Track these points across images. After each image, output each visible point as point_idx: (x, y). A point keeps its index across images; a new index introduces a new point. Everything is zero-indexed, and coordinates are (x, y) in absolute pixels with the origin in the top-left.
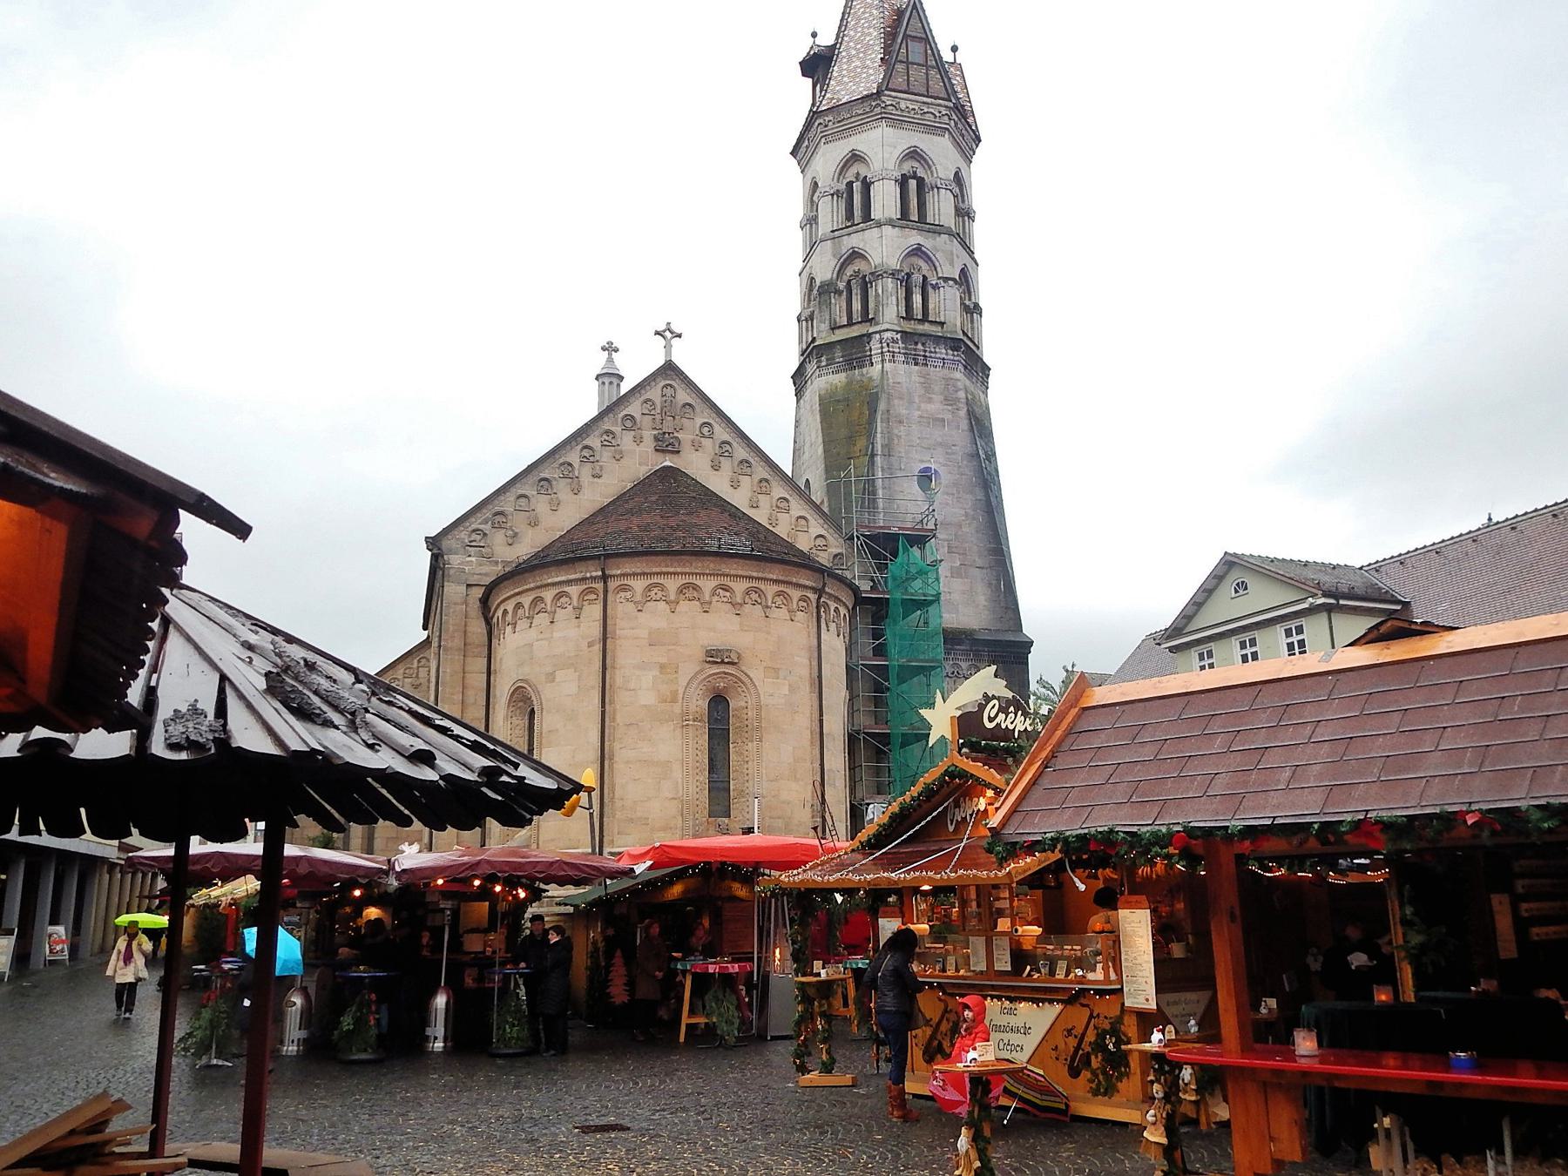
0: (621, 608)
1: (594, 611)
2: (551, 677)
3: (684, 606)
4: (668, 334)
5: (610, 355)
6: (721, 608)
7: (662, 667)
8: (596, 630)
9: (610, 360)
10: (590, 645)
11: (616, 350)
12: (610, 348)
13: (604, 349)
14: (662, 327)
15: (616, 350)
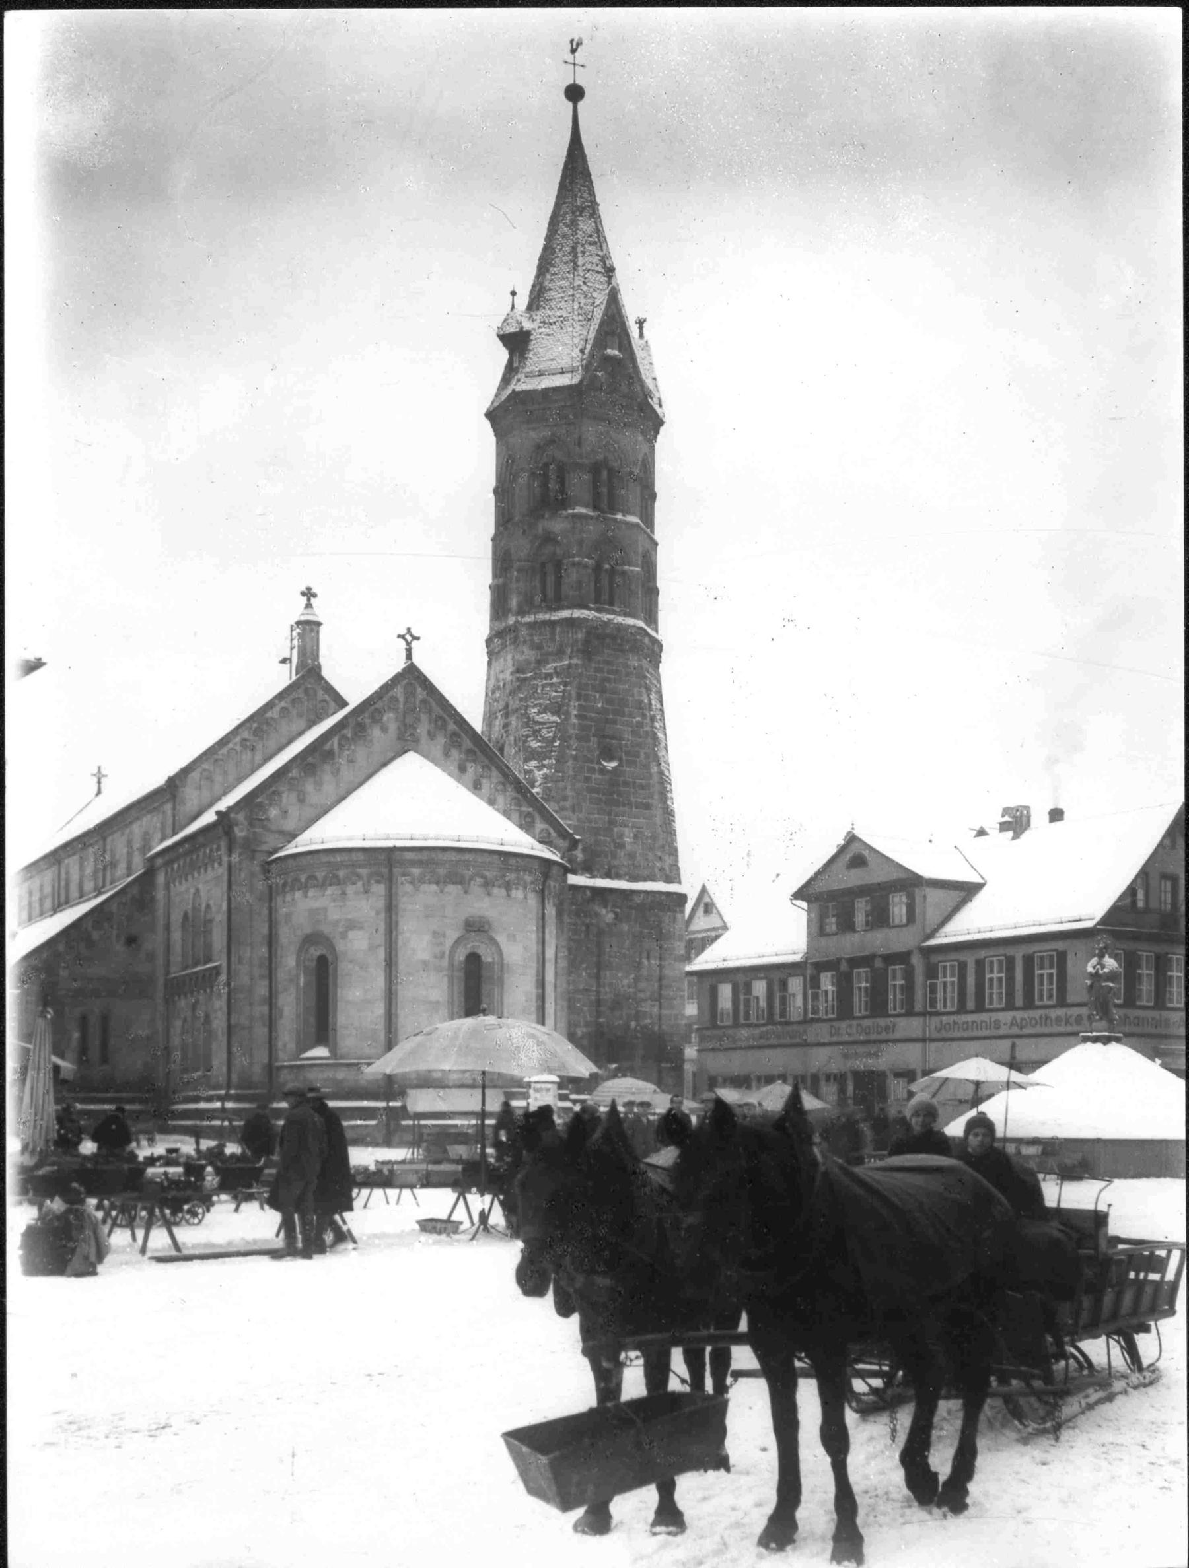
0: (405, 888)
1: (380, 889)
2: (344, 936)
3: (451, 888)
4: (409, 638)
5: (309, 600)
6: (476, 887)
7: (435, 934)
8: (381, 904)
9: (309, 606)
10: (378, 913)
11: (315, 596)
12: (309, 594)
13: (303, 594)
14: (403, 632)
15: (315, 596)
